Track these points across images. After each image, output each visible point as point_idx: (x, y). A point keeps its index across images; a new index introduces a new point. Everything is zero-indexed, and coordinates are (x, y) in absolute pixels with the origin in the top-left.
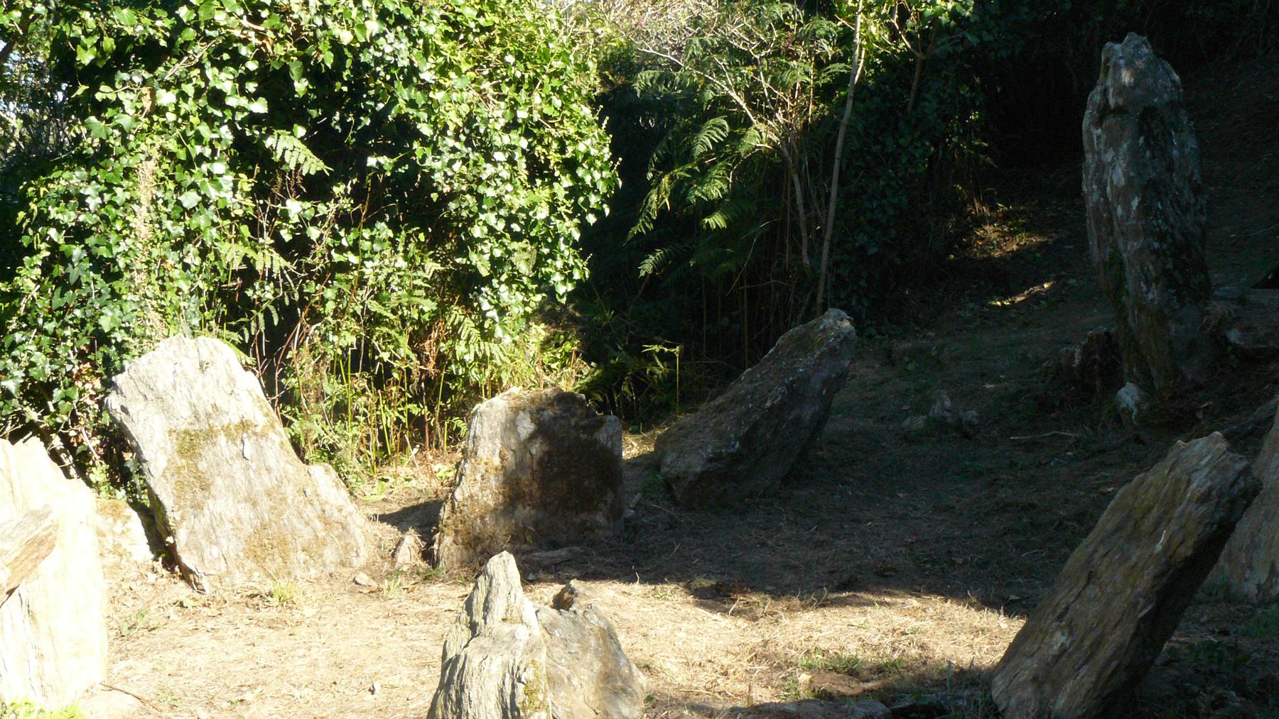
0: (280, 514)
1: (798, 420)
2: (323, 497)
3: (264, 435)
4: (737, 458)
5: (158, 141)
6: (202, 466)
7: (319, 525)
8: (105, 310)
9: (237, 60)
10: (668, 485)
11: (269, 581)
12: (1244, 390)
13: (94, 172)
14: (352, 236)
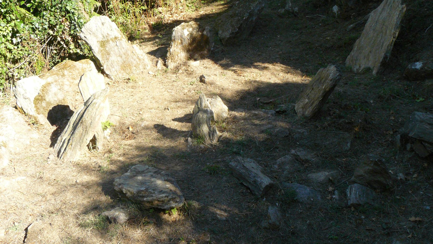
0: (128, 59)
1: (252, 20)
2: (137, 53)
3: (121, 40)
4: (237, 33)
6: (107, 49)
7: (137, 60)
10: (221, 40)
11: (128, 75)
12: (363, 9)
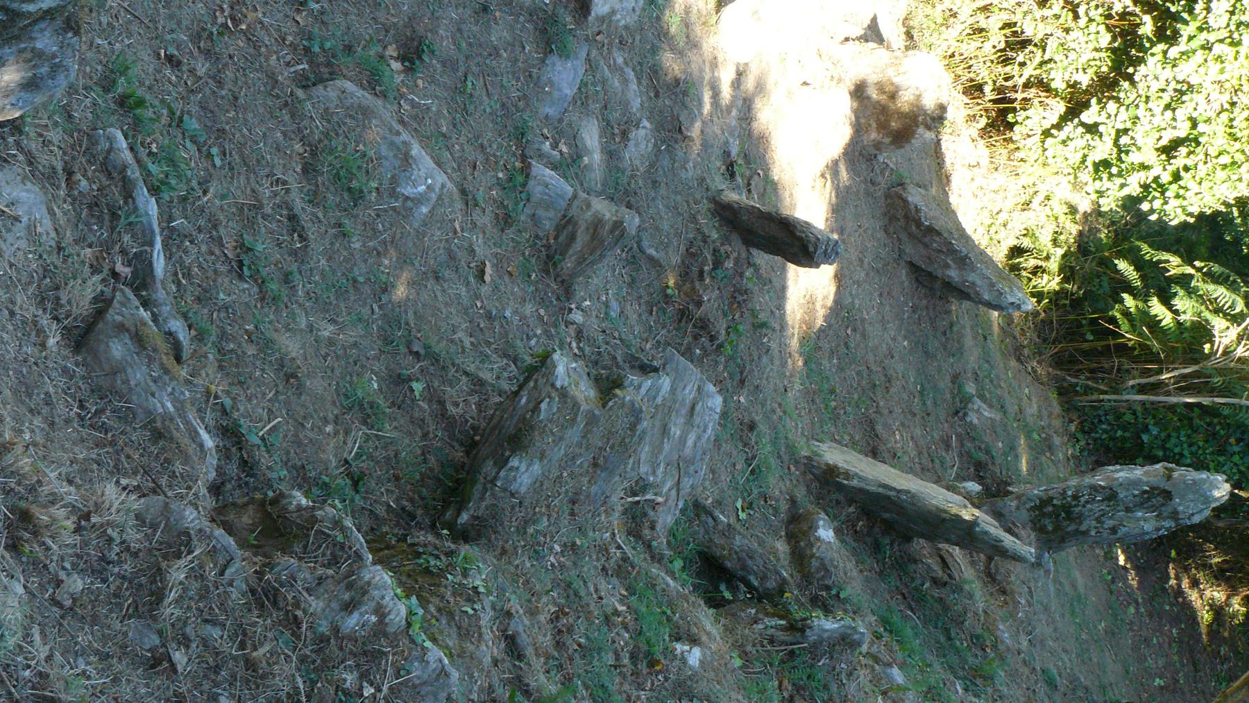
1: (947, 266)
4: (919, 223)
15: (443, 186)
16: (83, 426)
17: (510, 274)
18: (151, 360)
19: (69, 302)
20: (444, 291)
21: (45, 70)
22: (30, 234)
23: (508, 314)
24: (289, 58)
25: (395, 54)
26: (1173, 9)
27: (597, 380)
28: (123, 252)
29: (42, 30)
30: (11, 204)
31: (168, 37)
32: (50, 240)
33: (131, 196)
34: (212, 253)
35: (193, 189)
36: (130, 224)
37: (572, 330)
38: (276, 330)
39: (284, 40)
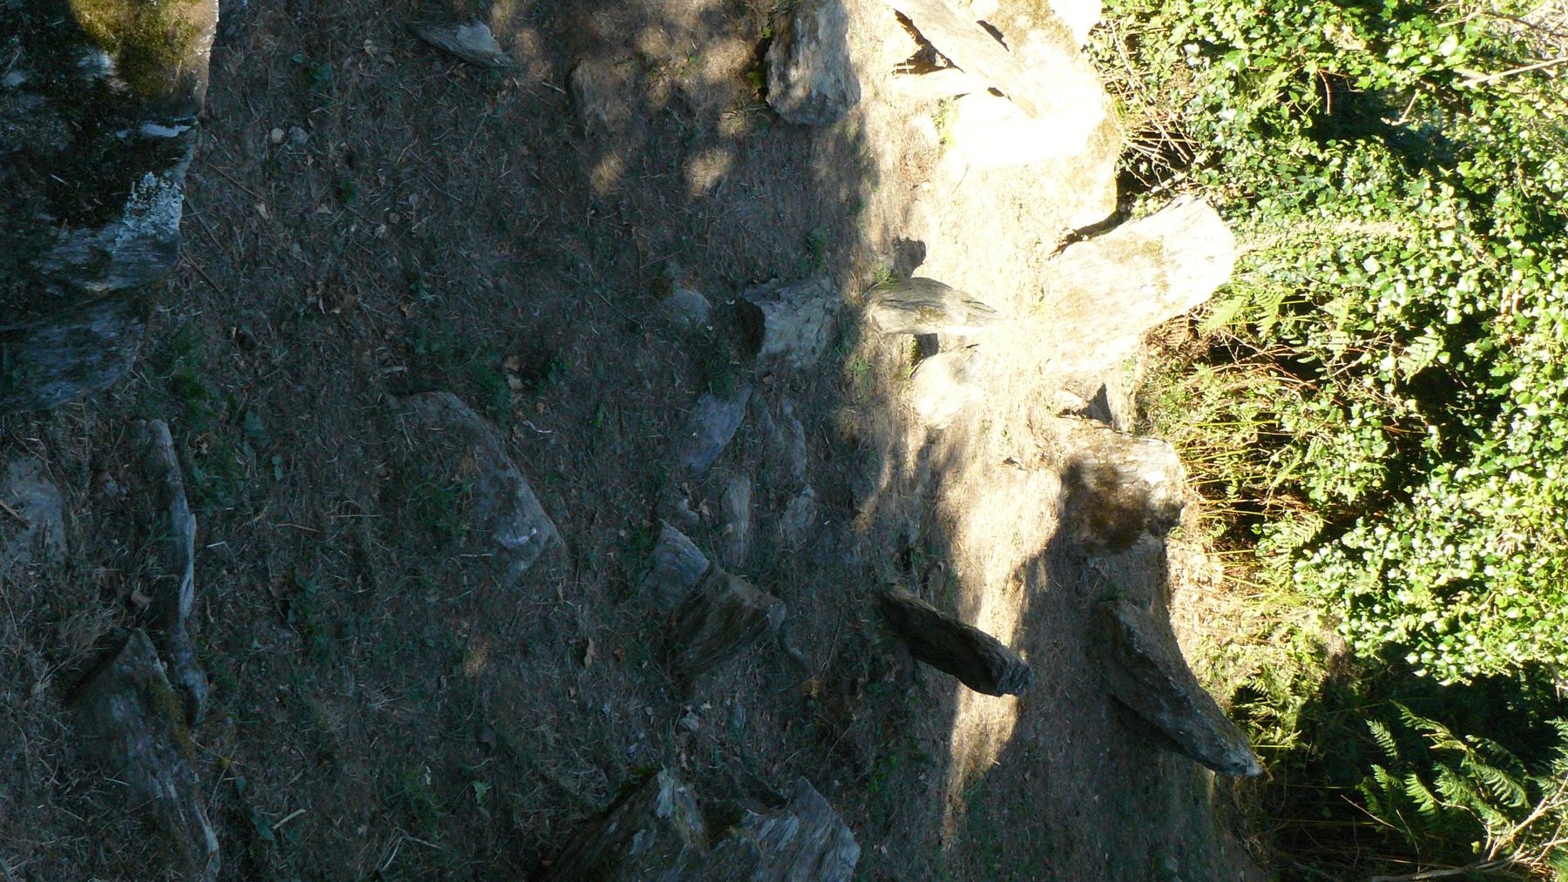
1: (1160, 708)
4: (1129, 649)
5: (1414, 236)
6: (1137, 258)
8: (1276, 203)
9: (1486, 292)
13: (1387, 188)
14: (1374, 421)
15: (550, 539)
16: (58, 803)
17: (617, 659)
18: (159, 729)
19: (69, 638)
20: (532, 670)
21: (96, 358)
22: (36, 545)
23: (607, 708)
24: (385, 356)
25: (515, 368)
26: (1466, 423)
27: (708, 812)
28: (145, 577)
29: (102, 311)
30: (19, 505)
31: (244, 312)
32: (58, 555)
33: (167, 509)
34: (253, 588)
35: (242, 505)
36: (159, 543)
37: (683, 738)
38: (317, 695)
39: (383, 333)
